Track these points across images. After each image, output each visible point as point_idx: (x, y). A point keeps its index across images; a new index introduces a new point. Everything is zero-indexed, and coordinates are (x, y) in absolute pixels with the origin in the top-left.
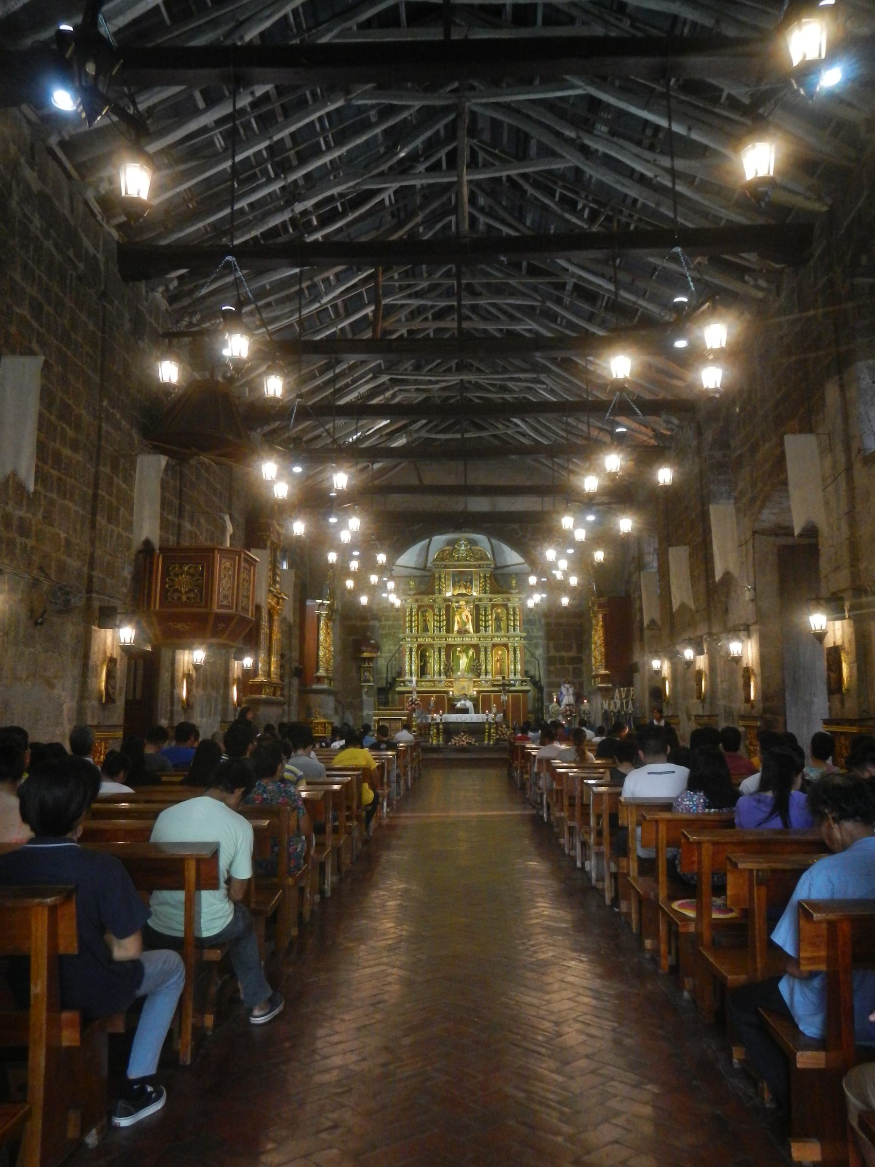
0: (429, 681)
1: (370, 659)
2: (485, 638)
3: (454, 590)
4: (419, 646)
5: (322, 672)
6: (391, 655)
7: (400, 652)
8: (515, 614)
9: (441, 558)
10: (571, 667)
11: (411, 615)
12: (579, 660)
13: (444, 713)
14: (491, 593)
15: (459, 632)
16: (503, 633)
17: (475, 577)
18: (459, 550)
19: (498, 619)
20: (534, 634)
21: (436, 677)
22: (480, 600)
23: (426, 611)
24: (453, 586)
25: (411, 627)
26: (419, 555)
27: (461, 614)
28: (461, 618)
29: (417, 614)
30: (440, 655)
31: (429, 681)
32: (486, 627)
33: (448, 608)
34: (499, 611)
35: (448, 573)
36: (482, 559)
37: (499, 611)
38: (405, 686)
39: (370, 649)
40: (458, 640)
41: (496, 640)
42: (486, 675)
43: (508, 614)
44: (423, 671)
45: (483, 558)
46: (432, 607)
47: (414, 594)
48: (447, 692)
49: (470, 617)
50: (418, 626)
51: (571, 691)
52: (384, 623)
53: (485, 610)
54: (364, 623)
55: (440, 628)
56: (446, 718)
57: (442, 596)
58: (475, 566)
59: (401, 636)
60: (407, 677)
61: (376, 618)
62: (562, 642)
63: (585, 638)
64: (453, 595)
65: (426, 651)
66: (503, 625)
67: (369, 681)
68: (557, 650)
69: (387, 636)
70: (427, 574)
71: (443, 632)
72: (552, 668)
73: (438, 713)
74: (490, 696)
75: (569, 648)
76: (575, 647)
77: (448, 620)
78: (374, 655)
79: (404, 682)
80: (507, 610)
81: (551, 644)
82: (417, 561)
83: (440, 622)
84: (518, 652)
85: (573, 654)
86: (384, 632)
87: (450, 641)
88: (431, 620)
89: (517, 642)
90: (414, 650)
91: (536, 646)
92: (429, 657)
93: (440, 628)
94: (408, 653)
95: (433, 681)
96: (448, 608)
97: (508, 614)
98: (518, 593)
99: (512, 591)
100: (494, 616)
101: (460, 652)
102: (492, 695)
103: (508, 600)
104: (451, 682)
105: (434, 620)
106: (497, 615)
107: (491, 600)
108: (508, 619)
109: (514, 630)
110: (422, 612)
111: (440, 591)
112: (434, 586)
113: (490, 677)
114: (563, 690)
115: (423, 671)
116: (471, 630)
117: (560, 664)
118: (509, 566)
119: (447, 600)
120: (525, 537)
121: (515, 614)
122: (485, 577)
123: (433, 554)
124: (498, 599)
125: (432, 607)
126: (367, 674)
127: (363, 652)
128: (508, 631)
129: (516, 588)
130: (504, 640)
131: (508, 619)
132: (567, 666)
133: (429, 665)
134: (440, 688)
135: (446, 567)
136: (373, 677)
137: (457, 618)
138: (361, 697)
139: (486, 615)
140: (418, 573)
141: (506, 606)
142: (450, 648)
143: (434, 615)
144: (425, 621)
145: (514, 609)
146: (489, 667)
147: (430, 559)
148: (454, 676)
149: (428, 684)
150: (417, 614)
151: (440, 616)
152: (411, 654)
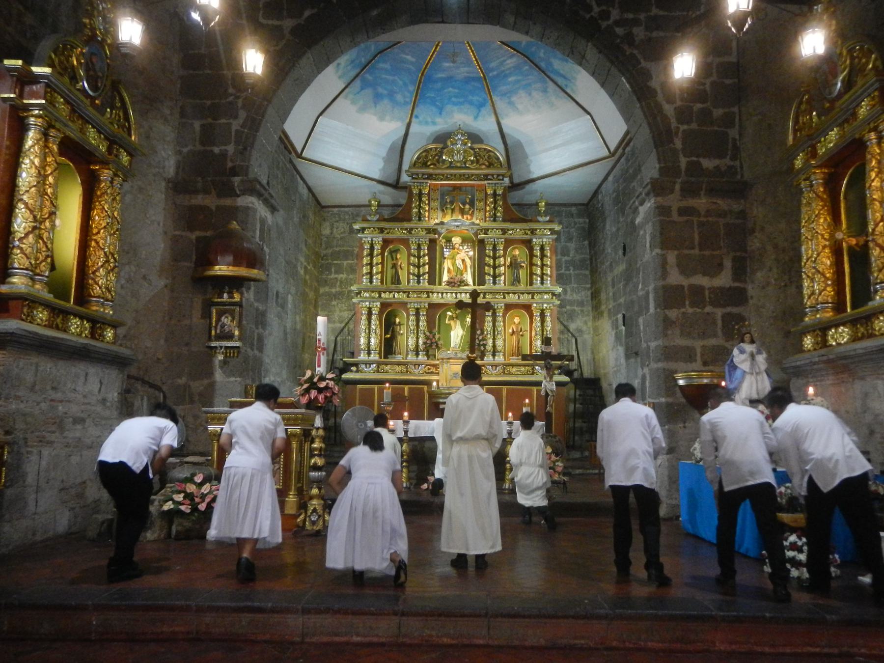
0: (399, 364)
1: (235, 283)
2: (494, 293)
3: (444, 216)
4: (384, 305)
5: (18, 282)
6: (343, 325)
7: (354, 317)
8: (543, 256)
9: (422, 161)
10: (719, 312)
11: (371, 255)
12: (737, 296)
13: (411, 417)
14: (504, 221)
15: (449, 283)
16: (522, 287)
17: (478, 195)
18: (453, 151)
19: (514, 265)
20: (568, 297)
21: (411, 358)
22: (486, 231)
23: (397, 251)
24: (443, 211)
25: (371, 274)
26: (387, 160)
27: (453, 258)
28: (454, 264)
29: (382, 254)
30: (418, 321)
31: (399, 364)
32: (495, 277)
33: (433, 242)
34: (517, 252)
35: (432, 189)
36: (490, 165)
37: (517, 252)
38: (357, 371)
39: (230, 258)
40: (450, 298)
41: (512, 298)
42: (494, 355)
43: (532, 256)
44: (389, 347)
45: (492, 162)
46: (405, 242)
47: (378, 220)
48: (428, 383)
49: (469, 262)
50: (382, 272)
51: (761, 359)
52: (333, 276)
53: (495, 249)
54: (228, 202)
55: (419, 276)
56: (417, 428)
57: (424, 224)
58: (478, 177)
59: (354, 288)
60: (363, 357)
61: (253, 188)
62: (696, 251)
63: (754, 243)
64: (442, 223)
65: (395, 317)
66: (523, 274)
67: (230, 337)
68: (684, 271)
69: (337, 296)
70: (401, 197)
71: (425, 284)
72: (673, 314)
73: (400, 417)
74: (501, 390)
75: (715, 269)
76: (728, 263)
77: (432, 264)
78: (243, 271)
79: (356, 364)
80: (531, 249)
81: (672, 257)
82: (384, 169)
83: (419, 267)
84: (548, 319)
85: (724, 280)
86: (334, 290)
87: (436, 298)
88: (405, 265)
89: (545, 302)
90: (375, 311)
91: (571, 316)
92: (400, 324)
93: (419, 276)
94: (364, 317)
95: (405, 364)
96: (433, 242)
97: (532, 256)
98: (550, 221)
99: (540, 219)
100: (509, 260)
101: (451, 318)
102: (505, 388)
103: (533, 231)
104: (434, 366)
105: (409, 264)
106: (514, 258)
107: (504, 231)
108: (532, 264)
109: (542, 283)
110: (391, 252)
111: (420, 217)
112: (410, 209)
113: (500, 359)
114: (741, 357)
115: (389, 347)
116: (470, 281)
117: (693, 304)
118: (533, 181)
119: (429, 231)
120: (605, 15)
121: (543, 256)
122: (495, 195)
123: (411, 154)
124: (517, 231)
125: (405, 242)
126: (226, 320)
127: (212, 263)
128: (531, 284)
129: (546, 214)
130: (525, 299)
131: (532, 264)
132: (708, 309)
133: (399, 338)
134: (416, 374)
135: (430, 177)
136: (240, 326)
137: (447, 264)
138: (210, 374)
139: (495, 258)
140: (388, 196)
141: (528, 243)
142: (433, 307)
143: (410, 255)
144: (394, 266)
145: (542, 249)
146: (499, 343)
147: (406, 166)
148: (439, 355)
149: (398, 368)
150: (382, 254)
151: (419, 257)
152: (369, 319)
